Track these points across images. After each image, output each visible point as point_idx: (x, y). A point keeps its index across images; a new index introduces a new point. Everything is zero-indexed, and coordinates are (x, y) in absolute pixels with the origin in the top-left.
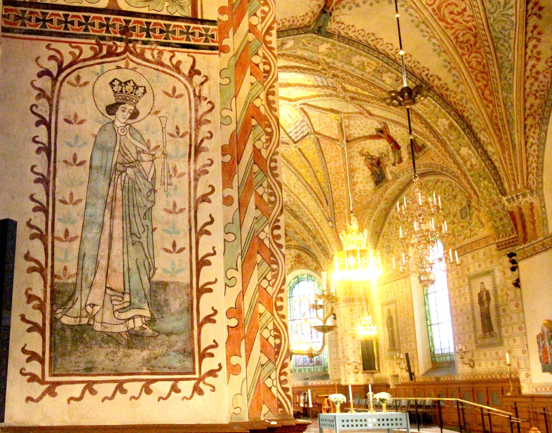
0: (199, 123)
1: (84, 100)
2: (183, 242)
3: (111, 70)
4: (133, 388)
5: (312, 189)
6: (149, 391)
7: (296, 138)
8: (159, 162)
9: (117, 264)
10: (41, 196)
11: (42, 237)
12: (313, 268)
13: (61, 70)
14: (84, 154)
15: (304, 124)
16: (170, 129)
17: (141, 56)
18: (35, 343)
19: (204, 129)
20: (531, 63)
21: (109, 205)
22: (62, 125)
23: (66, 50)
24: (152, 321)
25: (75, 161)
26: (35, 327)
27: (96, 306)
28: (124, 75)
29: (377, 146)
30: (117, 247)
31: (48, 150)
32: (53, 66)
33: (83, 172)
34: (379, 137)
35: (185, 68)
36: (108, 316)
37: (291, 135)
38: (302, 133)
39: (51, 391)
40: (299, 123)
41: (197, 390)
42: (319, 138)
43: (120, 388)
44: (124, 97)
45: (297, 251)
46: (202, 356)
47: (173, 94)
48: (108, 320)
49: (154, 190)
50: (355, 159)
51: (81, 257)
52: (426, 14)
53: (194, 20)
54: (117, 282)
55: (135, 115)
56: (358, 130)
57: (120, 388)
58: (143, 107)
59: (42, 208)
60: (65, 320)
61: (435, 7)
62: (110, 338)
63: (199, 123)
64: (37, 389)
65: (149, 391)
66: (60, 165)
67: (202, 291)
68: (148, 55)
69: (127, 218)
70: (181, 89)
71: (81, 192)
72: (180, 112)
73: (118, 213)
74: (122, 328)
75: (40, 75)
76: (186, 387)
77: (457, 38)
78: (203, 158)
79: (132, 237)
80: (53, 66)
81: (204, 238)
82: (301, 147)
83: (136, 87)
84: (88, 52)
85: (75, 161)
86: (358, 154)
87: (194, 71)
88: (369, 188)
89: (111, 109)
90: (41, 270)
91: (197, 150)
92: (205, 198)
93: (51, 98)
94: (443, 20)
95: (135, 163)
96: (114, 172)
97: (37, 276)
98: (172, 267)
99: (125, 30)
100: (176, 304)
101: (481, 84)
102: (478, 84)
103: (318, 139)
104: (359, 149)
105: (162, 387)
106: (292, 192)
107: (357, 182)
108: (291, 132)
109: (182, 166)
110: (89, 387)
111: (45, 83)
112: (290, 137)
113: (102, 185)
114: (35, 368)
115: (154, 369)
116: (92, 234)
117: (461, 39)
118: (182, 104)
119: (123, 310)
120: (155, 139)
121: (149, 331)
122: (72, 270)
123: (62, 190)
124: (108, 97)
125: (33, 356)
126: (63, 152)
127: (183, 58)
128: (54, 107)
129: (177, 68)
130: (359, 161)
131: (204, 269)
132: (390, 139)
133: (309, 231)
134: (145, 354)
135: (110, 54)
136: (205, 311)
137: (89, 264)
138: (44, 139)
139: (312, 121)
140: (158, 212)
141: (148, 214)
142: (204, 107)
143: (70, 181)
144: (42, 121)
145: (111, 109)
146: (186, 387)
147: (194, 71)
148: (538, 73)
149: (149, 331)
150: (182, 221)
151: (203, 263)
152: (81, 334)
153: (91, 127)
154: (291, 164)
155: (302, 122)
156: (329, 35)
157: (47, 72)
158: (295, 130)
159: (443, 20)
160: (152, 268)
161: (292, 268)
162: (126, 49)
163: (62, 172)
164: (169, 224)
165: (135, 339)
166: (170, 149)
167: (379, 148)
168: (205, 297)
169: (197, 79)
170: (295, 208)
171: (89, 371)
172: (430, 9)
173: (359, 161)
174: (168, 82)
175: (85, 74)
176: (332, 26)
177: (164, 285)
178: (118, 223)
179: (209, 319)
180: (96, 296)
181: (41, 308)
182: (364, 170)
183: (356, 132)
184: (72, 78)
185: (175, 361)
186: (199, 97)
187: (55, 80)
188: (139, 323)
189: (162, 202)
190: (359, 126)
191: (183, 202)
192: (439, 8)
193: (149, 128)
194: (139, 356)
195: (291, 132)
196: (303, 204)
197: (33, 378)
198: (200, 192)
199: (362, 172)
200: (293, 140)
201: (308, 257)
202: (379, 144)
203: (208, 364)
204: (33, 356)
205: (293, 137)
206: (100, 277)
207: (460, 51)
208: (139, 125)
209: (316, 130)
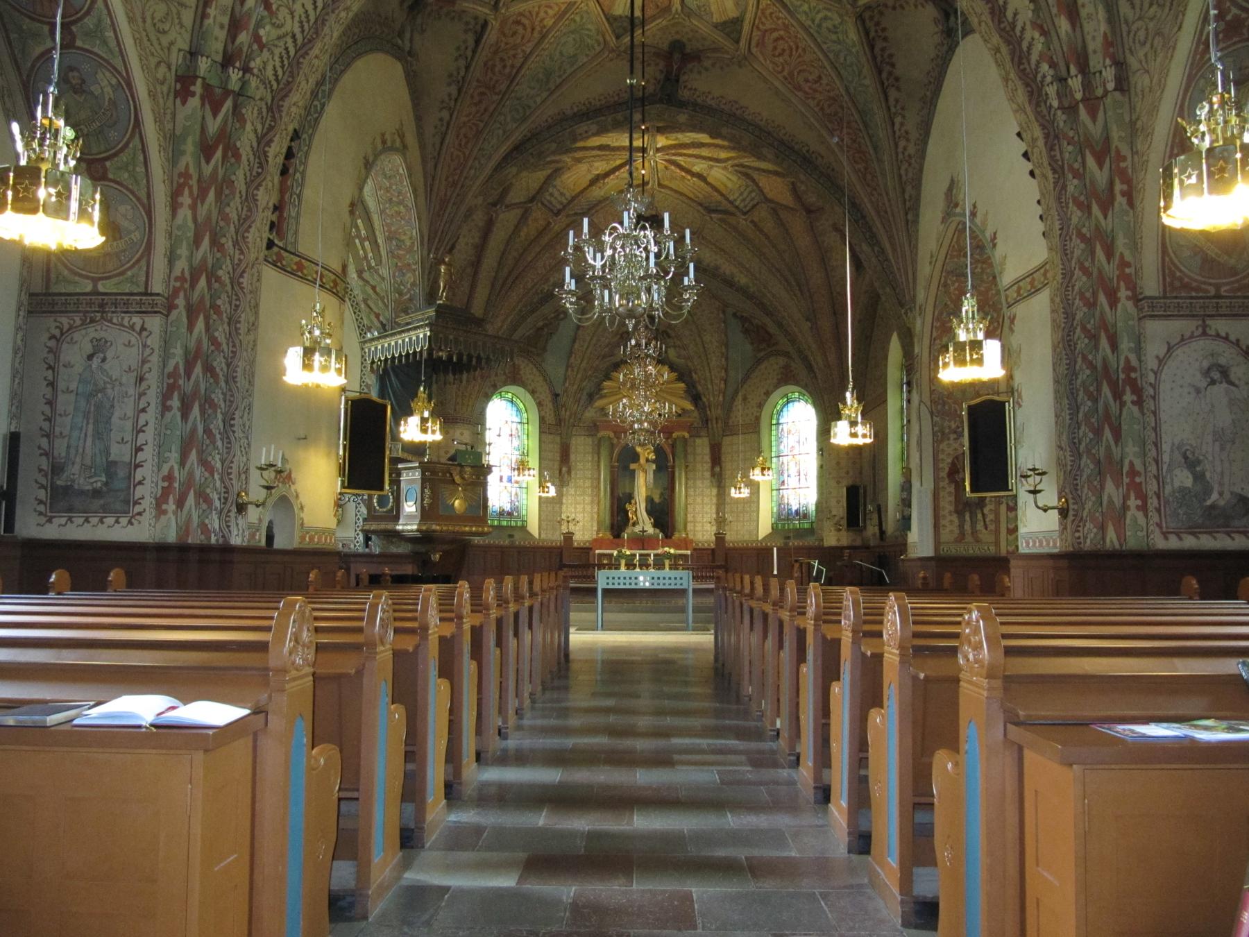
0: (144, 362)
1: (74, 354)
2: (128, 438)
3: (92, 332)
4: (94, 520)
6: (102, 522)
8: (116, 389)
9: (88, 451)
10: (48, 412)
11: (48, 436)
13: (62, 334)
14: (73, 386)
16: (125, 367)
17: (110, 321)
18: (42, 494)
19: (147, 366)
20: (902, 143)
21: (86, 416)
22: (62, 369)
23: (65, 321)
24: (106, 484)
25: (68, 391)
26: (42, 487)
27: (76, 475)
28: (102, 334)
30: (89, 440)
31: (52, 384)
32: (57, 332)
33: (72, 397)
35: (138, 328)
36: (82, 481)
39: (50, 520)
41: (130, 523)
42: (776, 209)
43: (87, 520)
44: (99, 348)
46: (136, 503)
47: (129, 345)
48: (83, 483)
49: (112, 406)
51: (68, 447)
52: (777, 84)
53: (146, 294)
54: (88, 462)
55: (104, 360)
57: (87, 520)
58: (109, 354)
59: (49, 419)
60: (59, 483)
61: (785, 73)
62: (82, 493)
63: (144, 362)
64: (43, 520)
65: (102, 522)
66: (59, 393)
67: (137, 466)
68: (115, 320)
69: (96, 422)
70: (133, 341)
71: (71, 409)
72: (131, 356)
73: (91, 421)
74: (89, 487)
75: (50, 339)
76: (124, 521)
77: (822, 109)
78: (144, 385)
79: (98, 435)
80: (57, 332)
81: (141, 435)
83: (106, 342)
84: (78, 322)
85: (68, 391)
87: (143, 329)
89: (90, 357)
90: (46, 454)
91: (141, 379)
92: (144, 410)
93: (54, 352)
94: (799, 88)
95: (103, 390)
96: (92, 395)
97: (44, 458)
98: (120, 453)
99: (102, 305)
100: (122, 473)
101: (861, 166)
102: (857, 166)
103: (774, 209)
105: (110, 520)
109: (131, 391)
110: (70, 519)
111: (52, 343)
112: (737, 207)
113: (83, 403)
114: (42, 508)
115: (106, 510)
116: (76, 434)
117: (828, 111)
118: (134, 350)
119: (90, 477)
120: (115, 374)
121: (104, 489)
122: (63, 454)
123: (60, 408)
124: (88, 349)
125: (41, 502)
126: (61, 385)
127: (137, 320)
128: (57, 358)
129: (132, 327)
131: (140, 454)
134: (102, 502)
135: (92, 321)
136: (138, 478)
137: (73, 451)
138: (50, 378)
140: (115, 420)
141: (108, 421)
142: (148, 351)
143: (65, 402)
144: (50, 367)
145: (90, 357)
146: (124, 521)
147: (143, 329)
148: (909, 156)
149: (104, 489)
150: (128, 425)
151: (139, 449)
152: (67, 490)
153: (78, 368)
156: (682, 105)
157: (53, 337)
159: (799, 88)
160: (108, 454)
162: (102, 317)
163: (61, 398)
164: (121, 425)
165: (96, 493)
166: (124, 380)
168: (139, 470)
169: (145, 334)
171: (70, 510)
172: (779, 76)
174: (125, 337)
175: (77, 336)
176: (684, 94)
177: (115, 463)
178: (91, 427)
179: (140, 483)
180: (77, 467)
181: (46, 476)
184: (68, 339)
185: (118, 506)
186: (145, 346)
187: (58, 341)
188: (99, 484)
189: (117, 414)
191: (130, 413)
192: (791, 74)
193: (114, 368)
194: (99, 503)
197: (41, 514)
198: (141, 406)
203: (137, 509)
204: (41, 502)
206: (78, 460)
207: (830, 126)
208: (106, 366)
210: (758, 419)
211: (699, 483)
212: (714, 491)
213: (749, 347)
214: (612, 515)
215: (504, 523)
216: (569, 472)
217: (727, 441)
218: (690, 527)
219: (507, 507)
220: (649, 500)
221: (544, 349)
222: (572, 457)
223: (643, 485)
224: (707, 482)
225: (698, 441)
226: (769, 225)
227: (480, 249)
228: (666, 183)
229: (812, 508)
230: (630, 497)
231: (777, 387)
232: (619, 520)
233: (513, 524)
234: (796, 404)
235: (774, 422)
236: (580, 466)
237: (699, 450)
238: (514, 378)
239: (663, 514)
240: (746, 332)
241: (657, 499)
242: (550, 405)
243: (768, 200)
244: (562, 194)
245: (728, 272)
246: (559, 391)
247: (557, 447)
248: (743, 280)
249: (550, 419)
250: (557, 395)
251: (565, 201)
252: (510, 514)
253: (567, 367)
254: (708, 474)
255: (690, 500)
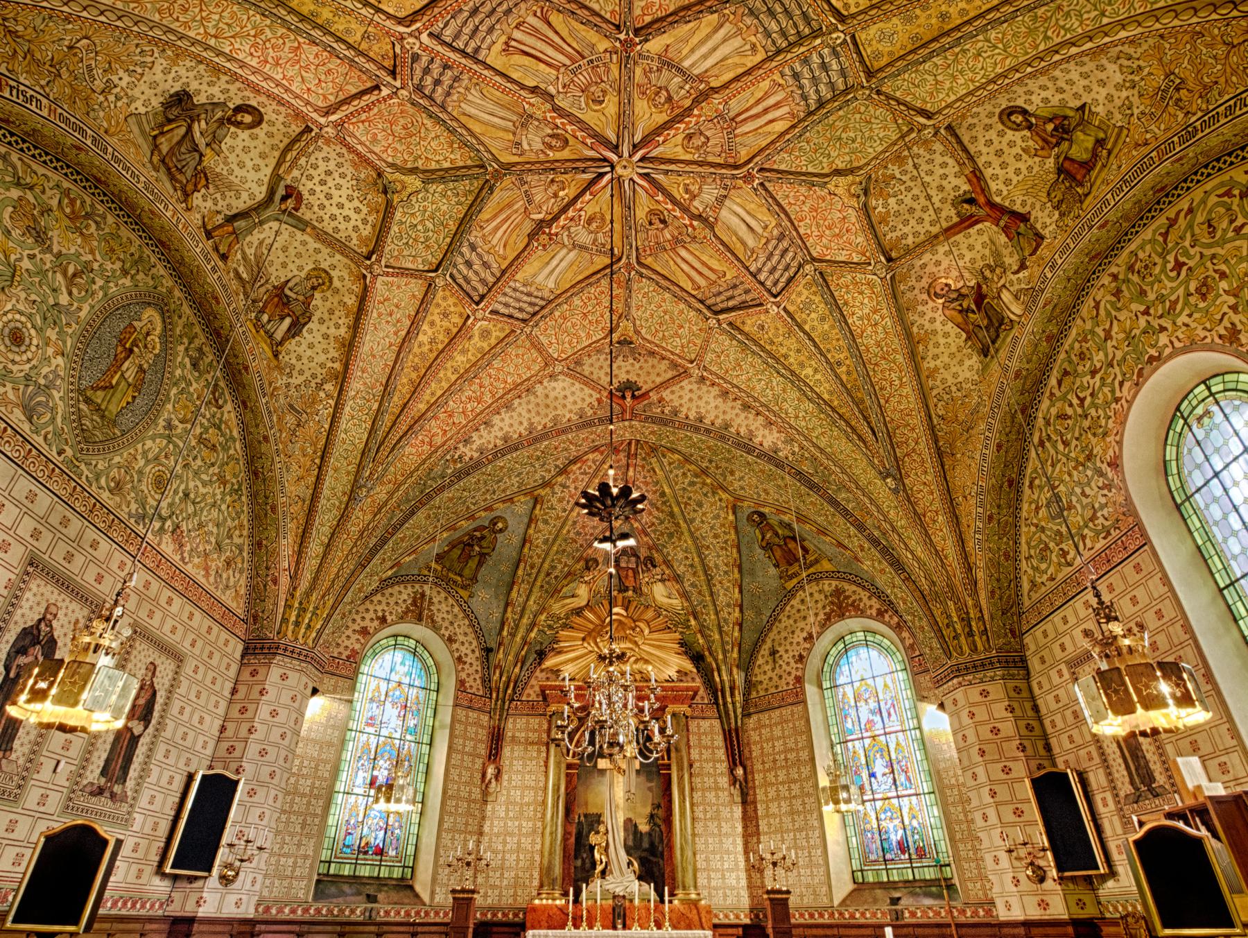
5: (833, 409)
7: (775, 284)
12: (874, 612)
15: (785, 244)
29: (968, 256)
34: (966, 222)
37: (762, 277)
38: (787, 268)
40: (774, 242)
45: (834, 583)
50: (920, 308)
56: (913, 222)
82: (791, 308)
86: (925, 296)
88: (968, 375)
104: (924, 283)
106: (791, 427)
107: (936, 369)
108: (760, 270)
130: (930, 315)
132: (998, 211)
133: (846, 513)
139: (802, 231)
154: (777, 360)
155: (781, 237)
158: (769, 265)
161: (828, 618)
167: (973, 261)
170: (806, 468)
173: (930, 315)
182: (946, 335)
183: (906, 230)
190: (911, 210)
195: (760, 270)
196: (822, 451)
199: (942, 341)
200: (769, 291)
201: (859, 590)
202: (971, 248)
205: (769, 283)
209: (815, 254)
210: (799, 680)
211: (711, 796)
212: (738, 811)
213: (773, 571)
214: (566, 858)
215: (365, 871)
216: (498, 776)
217: (752, 722)
218: (702, 881)
219: (377, 838)
220: (630, 826)
221: (474, 579)
222: (506, 751)
223: (618, 798)
224: (724, 796)
225: (705, 724)
226: (816, 320)
227: (349, 347)
228: (649, 261)
229: (938, 836)
230: (594, 821)
231: (824, 625)
232: (578, 862)
233: (384, 873)
234: (863, 651)
235: (826, 684)
236: (518, 765)
237: (706, 741)
238: (418, 611)
239: (655, 858)
240: (768, 547)
241: (644, 828)
242: (477, 666)
243: (814, 259)
244: (486, 265)
245: (743, 431)
246: (493, 645)
247: (483, 734)
248: (768, 438)
249: (475, 685)
250: (488, 650)
251: (491, 280)
252: (380, 852)
253: (507, 605)
254: (724, 781)
255: (699, 828)
